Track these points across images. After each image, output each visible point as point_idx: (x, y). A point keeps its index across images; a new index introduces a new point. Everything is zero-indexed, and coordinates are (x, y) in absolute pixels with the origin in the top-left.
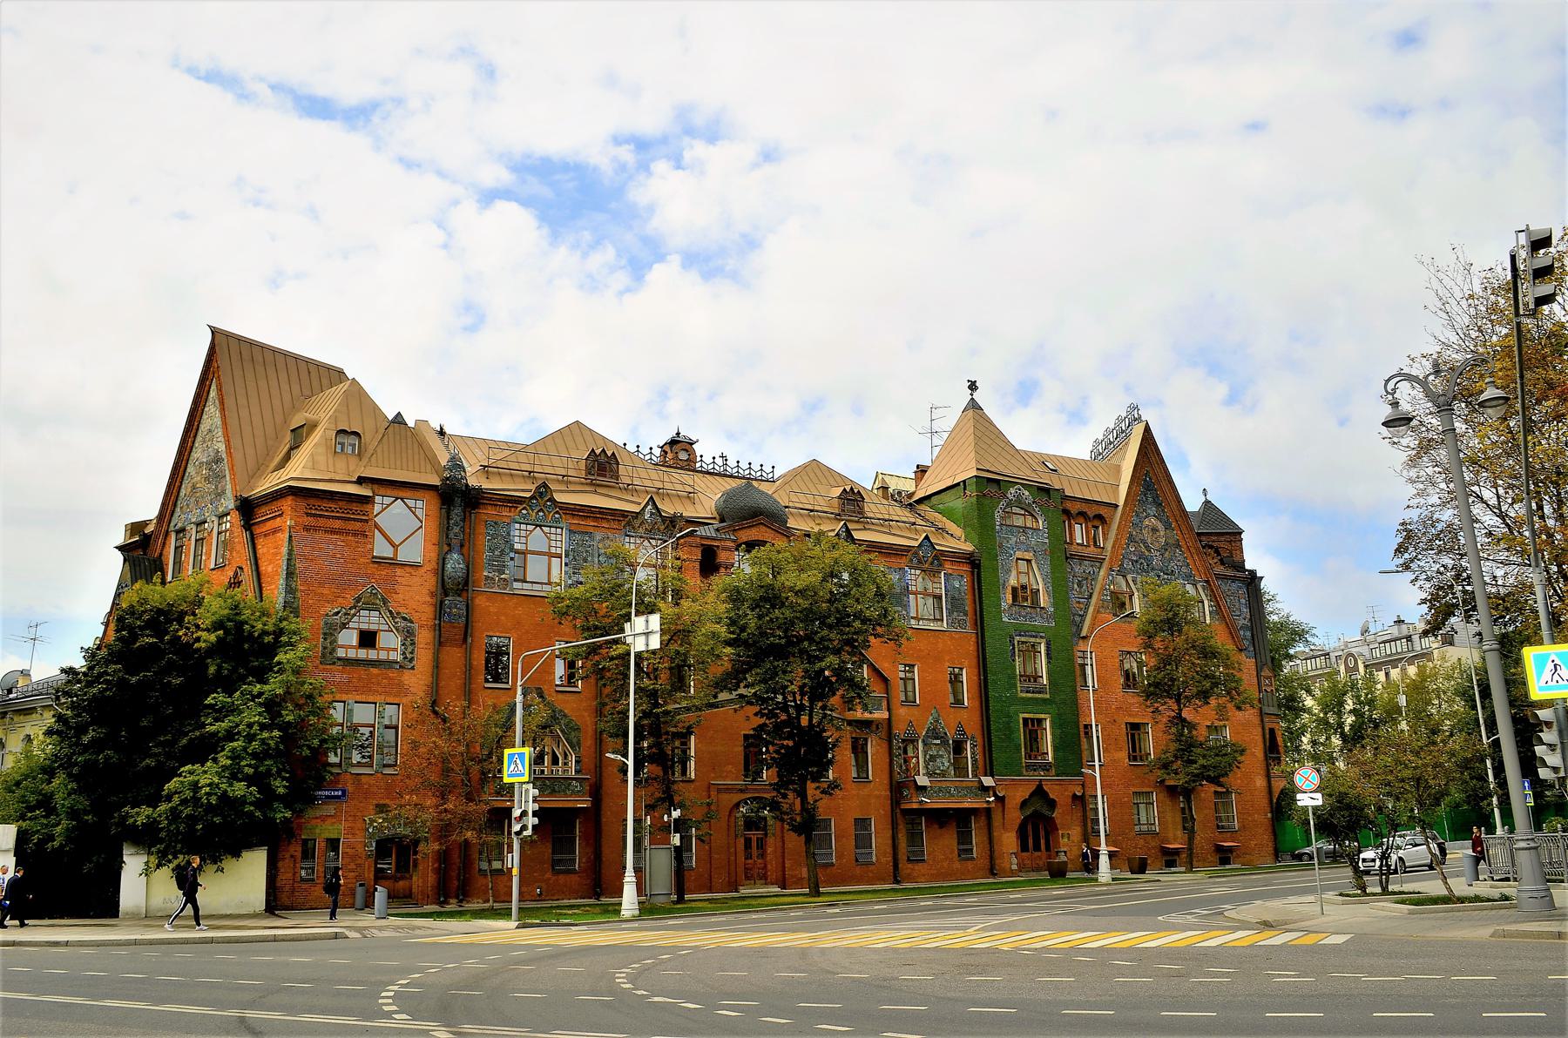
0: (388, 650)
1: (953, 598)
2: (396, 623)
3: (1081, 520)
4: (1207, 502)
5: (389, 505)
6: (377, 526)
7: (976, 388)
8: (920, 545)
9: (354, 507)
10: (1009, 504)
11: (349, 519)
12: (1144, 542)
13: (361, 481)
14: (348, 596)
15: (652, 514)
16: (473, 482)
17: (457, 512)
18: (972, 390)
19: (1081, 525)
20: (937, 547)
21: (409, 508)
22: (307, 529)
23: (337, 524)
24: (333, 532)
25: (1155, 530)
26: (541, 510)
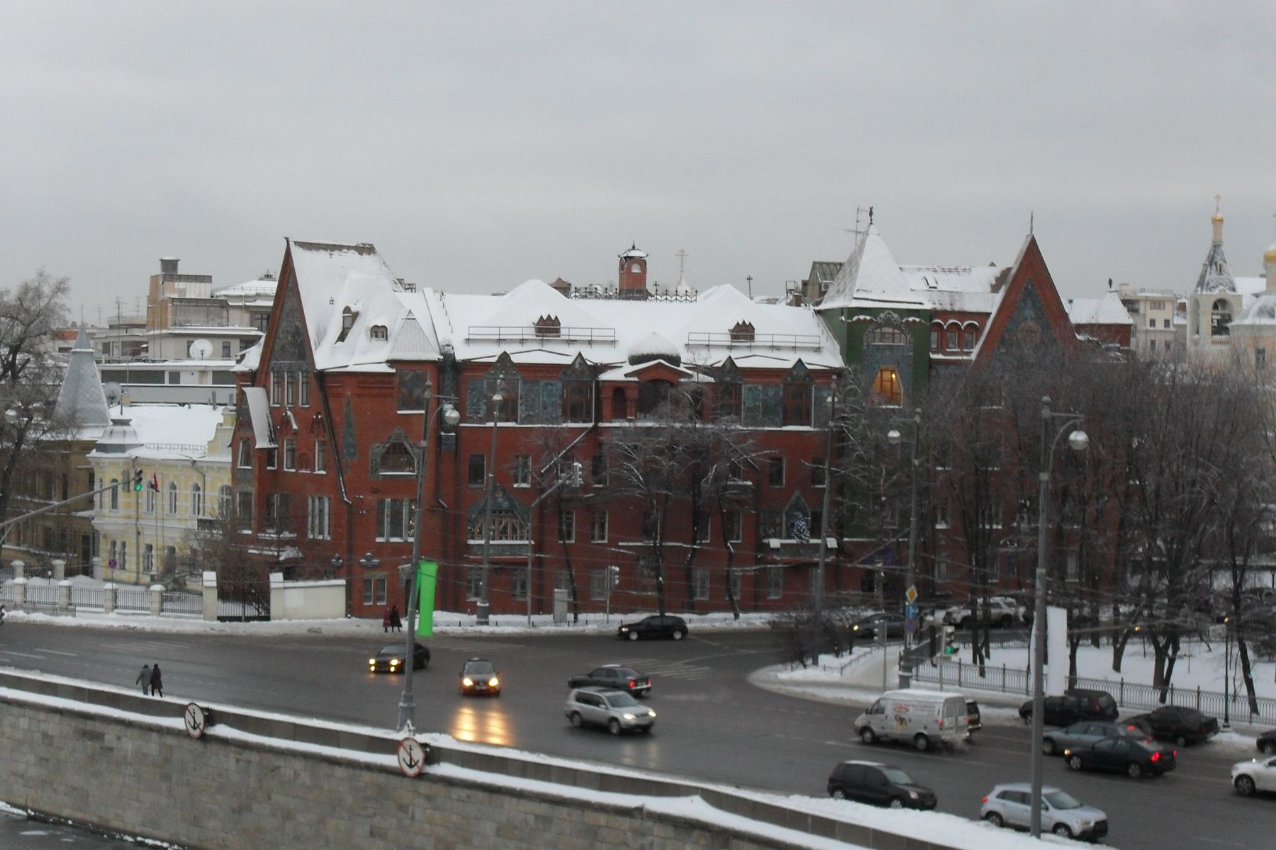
15: (580, 364)
22: (358, 395)
23: (376, 391)
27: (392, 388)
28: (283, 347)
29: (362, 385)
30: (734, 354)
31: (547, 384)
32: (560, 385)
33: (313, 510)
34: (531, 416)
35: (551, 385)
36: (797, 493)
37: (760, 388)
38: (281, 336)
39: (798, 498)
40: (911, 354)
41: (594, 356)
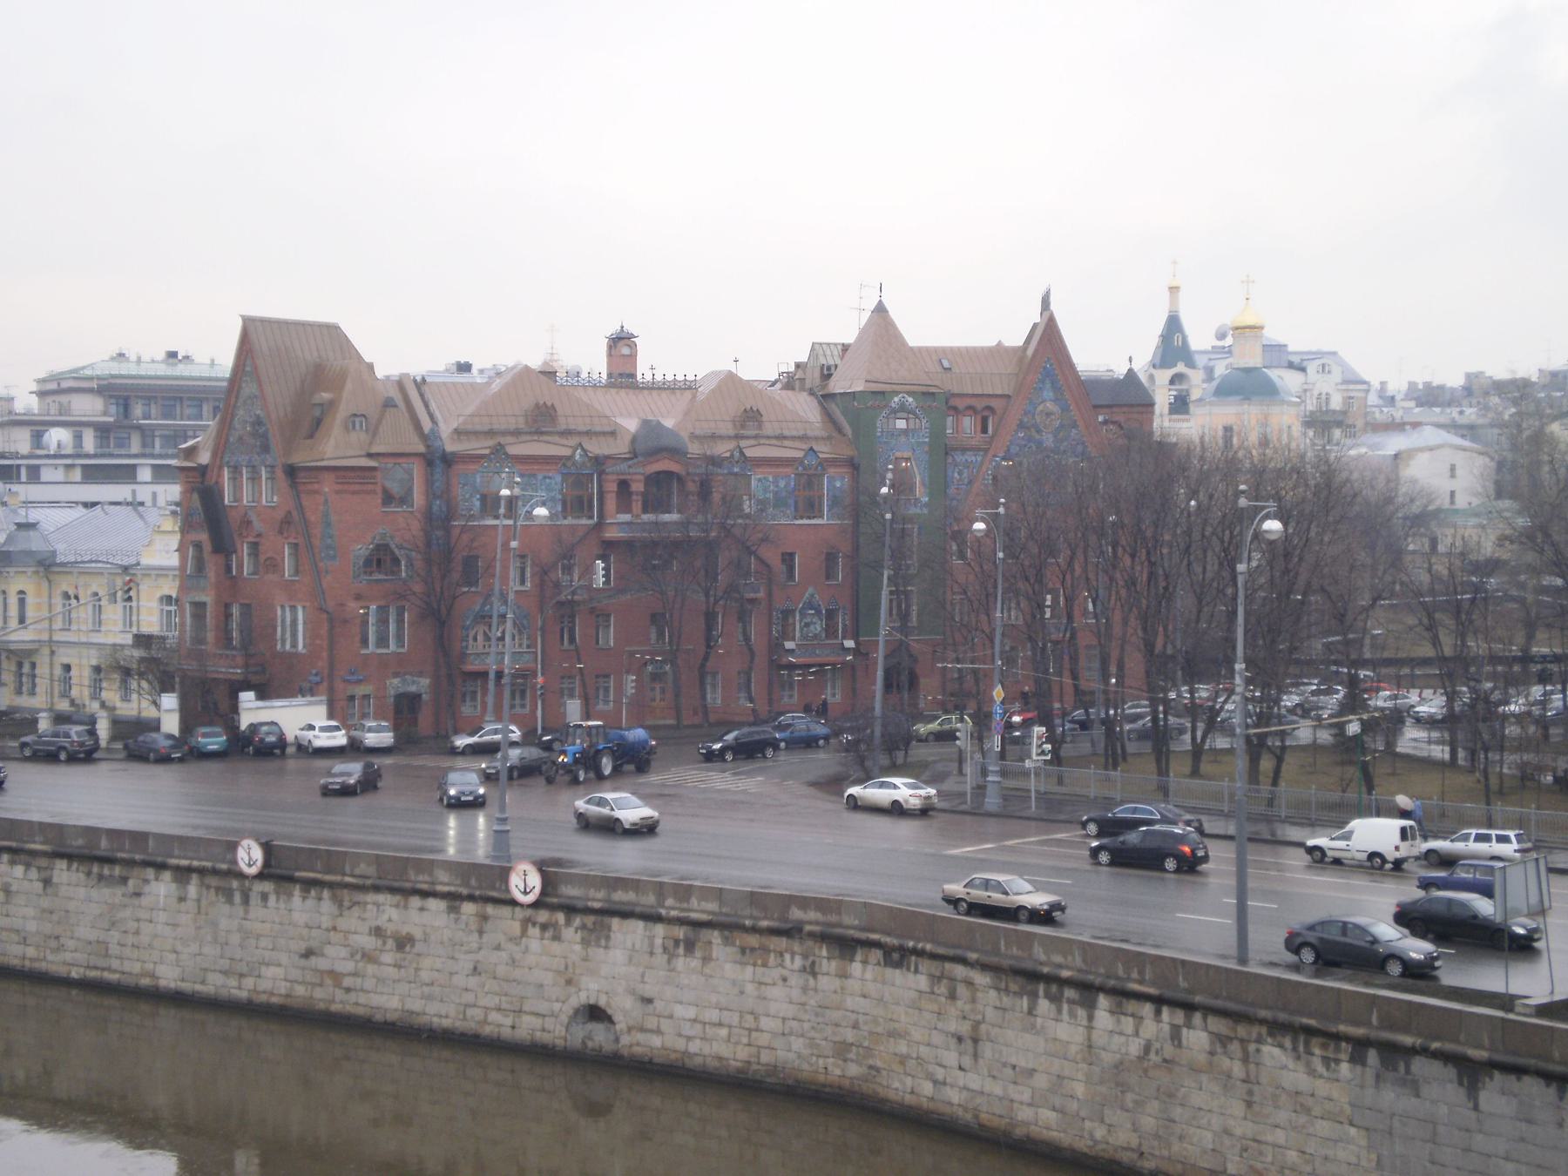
1: (835, 497)
3: (971, 412)
4: (1130, 371)
8: (805, 456)
9: (367, 474)
10: (894, 411)
11: (364, 483)
12: (1035, 426)
13: (370, 455)
16: (450, 448)
17: (439, 470)
20: (821, 456)
22: (337, 492)
23: (357, 487)
24: (354, 493)
25: (1048, 414)
27: (376, 483)
28: (240, 438)
29: (340, 481)
30: (743, 443)
31: (545, 478)
32: (559, 478)
33: (283, 621)
35: (550, 478)
36: (811, 590)
37: (771, 479)
38: (237, 426)
39: (812, 596)
40: (927, 440)
41: (597, 448)
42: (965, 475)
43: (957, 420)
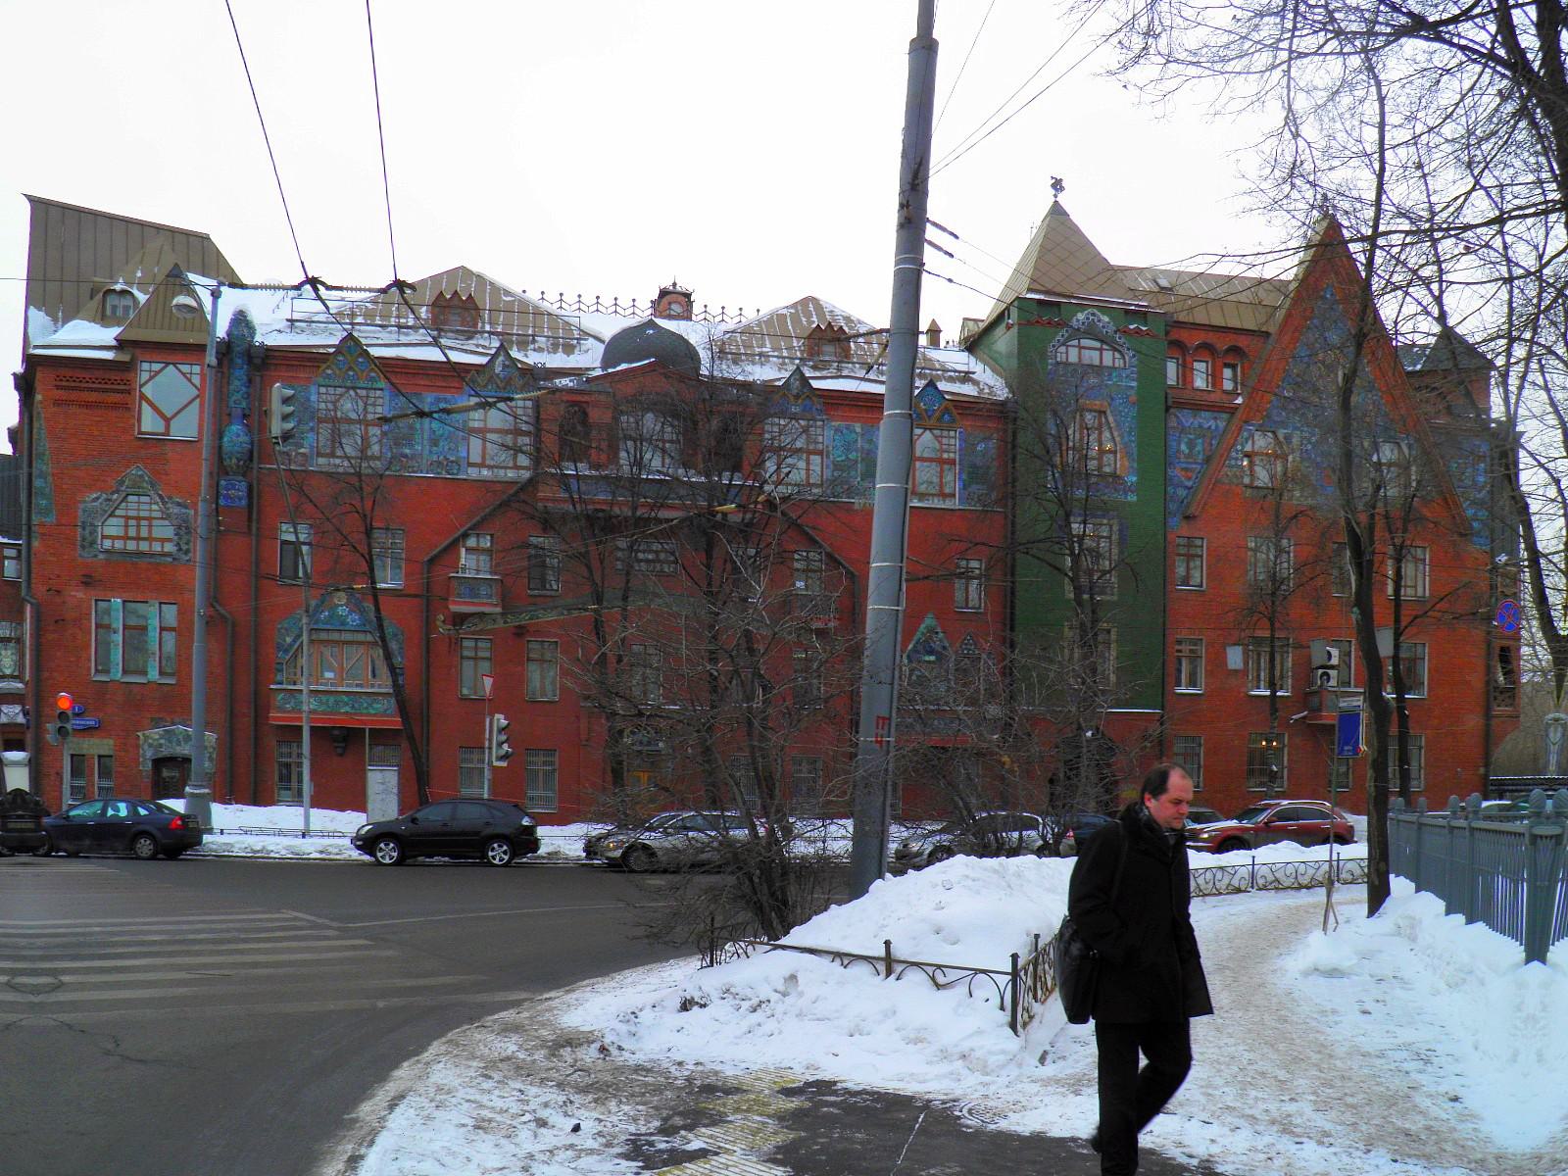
0: (163, 541)
2: (168, 509)
5: (158, 373)
6: (143, 397)
7: (1062, 189)
14: (109, 479)
15: (505, 366)
18: (1056, 190)
19: (1207, 362)
21: (183, 374)
23: (93, 397)
24: (88, 405)
26: (351, 368)
34: (406, 456)
36: (929, 621)
37: (858, 430)
39: (932, 631)
40: (1134, 384)
42: (1199, 448)
43: (1184, 366)
